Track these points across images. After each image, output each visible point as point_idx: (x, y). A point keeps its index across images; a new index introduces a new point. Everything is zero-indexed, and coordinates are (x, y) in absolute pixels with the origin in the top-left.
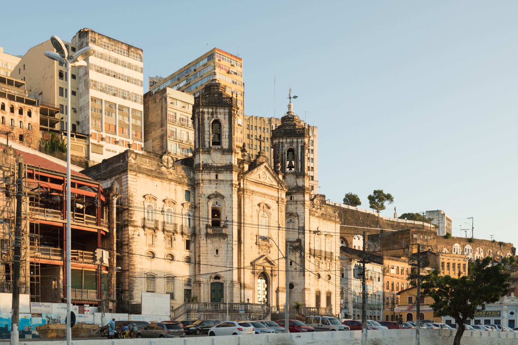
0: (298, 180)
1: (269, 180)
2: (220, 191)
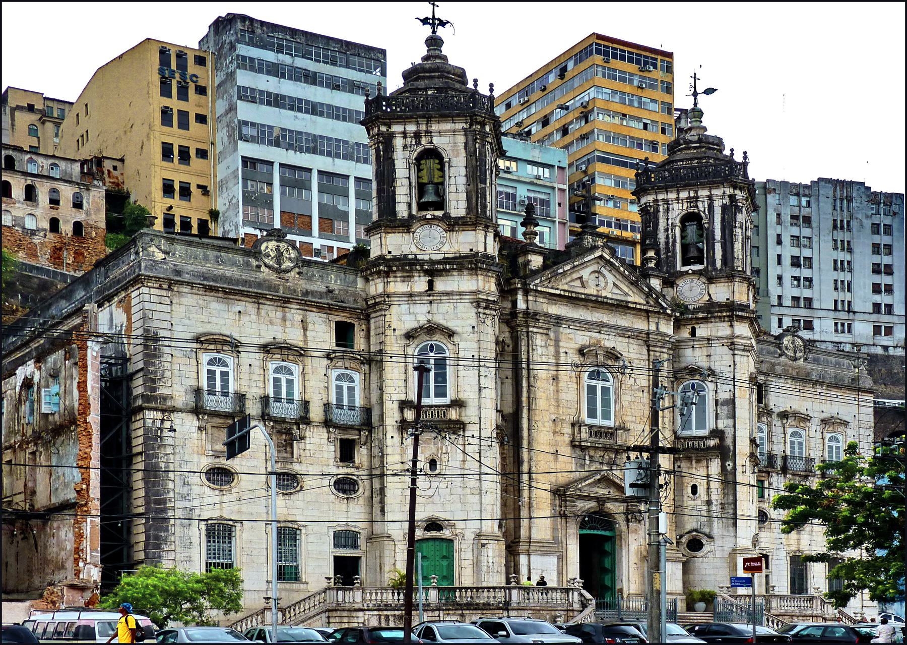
0: (712, 287)
1: (616, 291)
2: (439, 319)
